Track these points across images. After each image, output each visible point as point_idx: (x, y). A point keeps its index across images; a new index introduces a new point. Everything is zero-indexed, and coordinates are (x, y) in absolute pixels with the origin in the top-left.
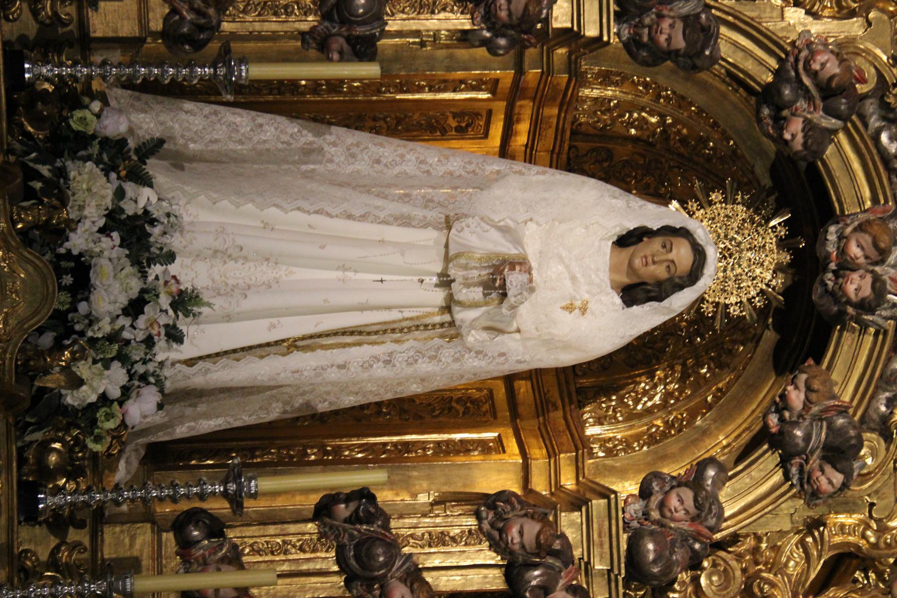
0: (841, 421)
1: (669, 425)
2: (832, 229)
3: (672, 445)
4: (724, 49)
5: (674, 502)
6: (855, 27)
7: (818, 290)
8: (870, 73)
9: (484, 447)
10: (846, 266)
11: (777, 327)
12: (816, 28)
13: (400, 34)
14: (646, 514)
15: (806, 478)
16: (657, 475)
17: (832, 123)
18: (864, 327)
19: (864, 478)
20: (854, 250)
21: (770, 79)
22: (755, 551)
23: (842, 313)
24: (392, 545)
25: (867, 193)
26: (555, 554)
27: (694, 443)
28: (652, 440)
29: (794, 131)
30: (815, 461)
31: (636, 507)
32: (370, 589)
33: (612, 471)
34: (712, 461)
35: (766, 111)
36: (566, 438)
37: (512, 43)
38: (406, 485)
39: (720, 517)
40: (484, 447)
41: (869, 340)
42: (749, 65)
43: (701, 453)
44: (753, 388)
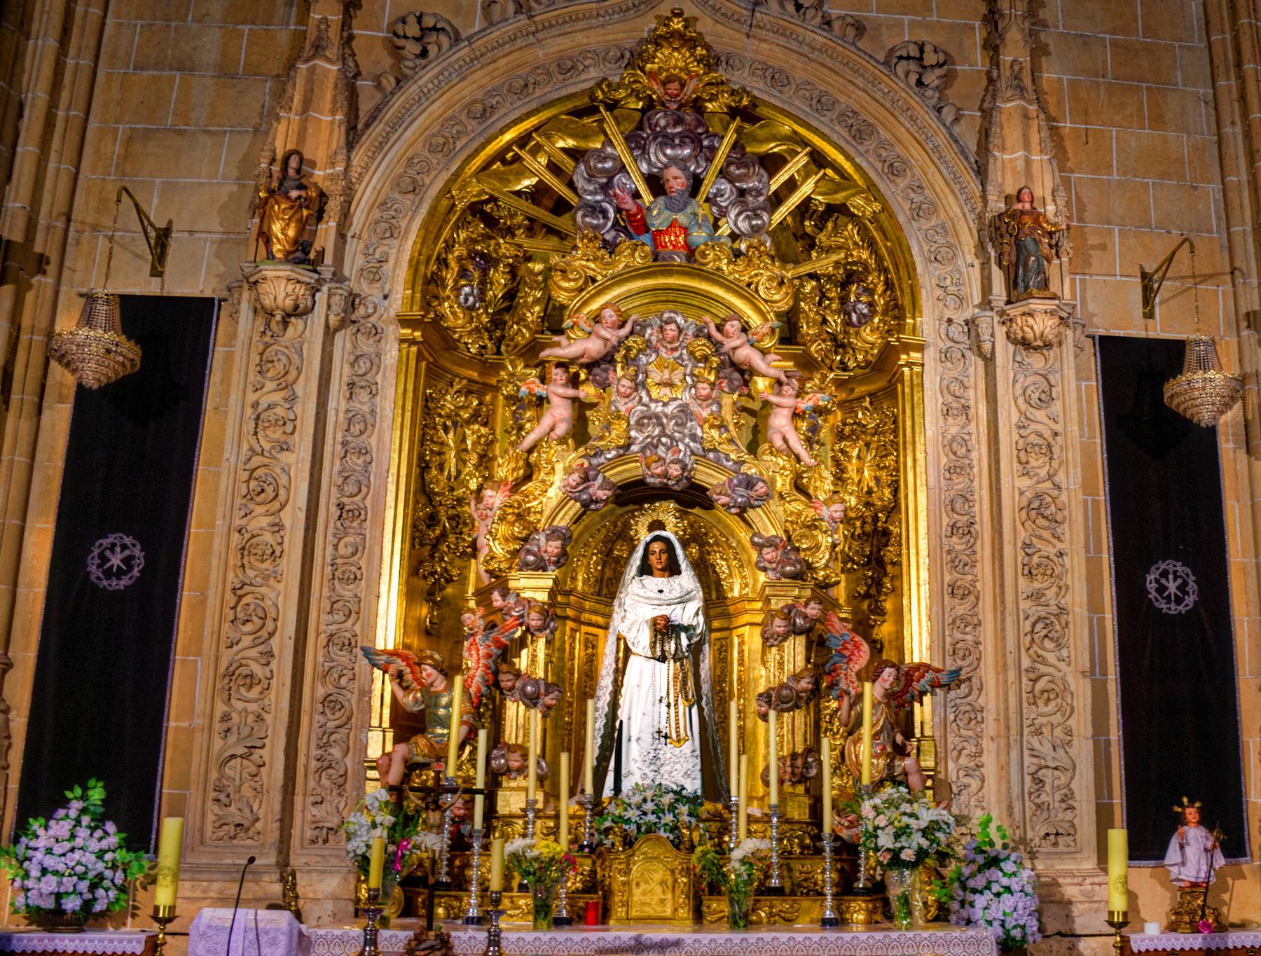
0: (735, 482)
1: (735, 558)
2: (649, 480)
3: (744, 557)
4: (563, 524)
5: (768, 557)
6: (559, 467)
7: (676, 487)
8: (580, 461)
9: (741, 644)
10: (665, 475)
11: (693, 507)
12: (557, 483)
13: (546, 672)
14: (774, 570)
15: (760, 498)
16: (757, 564)
17: (600, 478)
18: (693, 469)
19: (761, 473)
20: (658, 471)
21: (578, 504)
22: (792, 522)
23: (687, 478)
24: (783, 686)
25: (633, 465)
26: (790, 612)
27: (743, 547)
28: (741, 566)
29: (603, 494)
30: (752, 493)
31: (770, 574)
32: (801, 698)
33: (754, 585)
34: (751, 539)
35: (593, 507)
36: (739, 606)
37: (552, 619)
38: (756, 680)
39: (776, 537)
40: (741, 644)
41: (699, 467)
42: (571, 513)
43: (748, 545)
44: (720, 521)
